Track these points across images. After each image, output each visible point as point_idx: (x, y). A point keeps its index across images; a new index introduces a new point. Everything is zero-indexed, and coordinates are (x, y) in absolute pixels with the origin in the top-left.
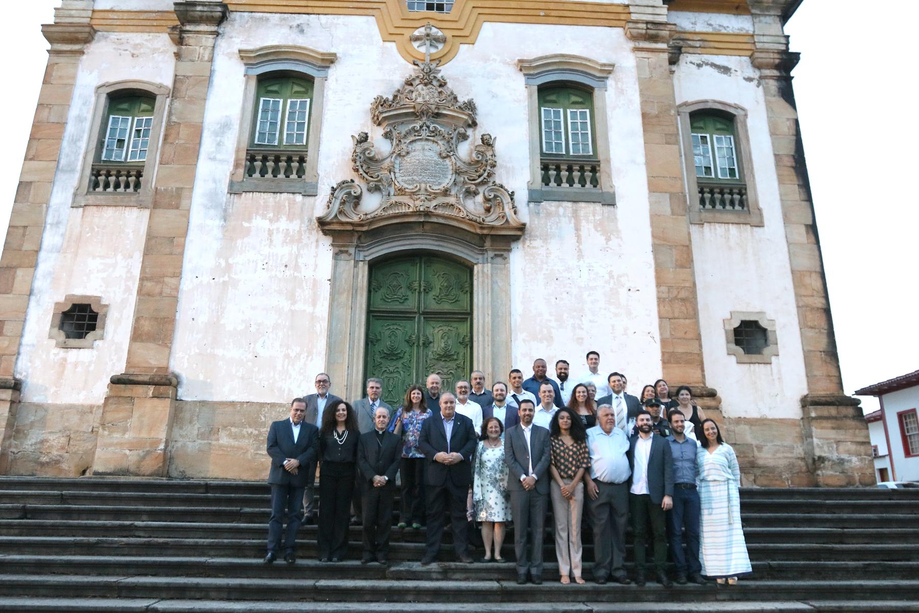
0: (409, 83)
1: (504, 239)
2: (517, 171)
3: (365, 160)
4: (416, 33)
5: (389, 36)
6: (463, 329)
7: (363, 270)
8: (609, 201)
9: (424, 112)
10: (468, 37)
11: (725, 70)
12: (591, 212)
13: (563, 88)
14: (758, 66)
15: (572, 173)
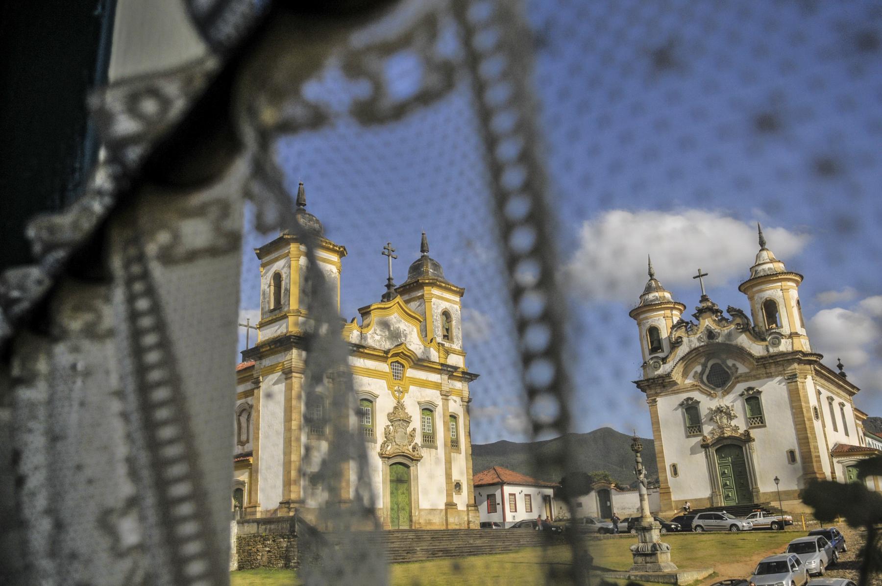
0: (395, 408)
1: (416, 460)
2: (418, 440)
3: (387, 434)
4: (396, 388)
5: (389, 388)
6: (406, 485)
7: (388, 468)
8: (436, 448)
9: (398, 417)
10: (407, 391)
11: (455, 401)
12: (434, 450)
13: (428, 410)
14: (462, 401)
15: (429, 439)
